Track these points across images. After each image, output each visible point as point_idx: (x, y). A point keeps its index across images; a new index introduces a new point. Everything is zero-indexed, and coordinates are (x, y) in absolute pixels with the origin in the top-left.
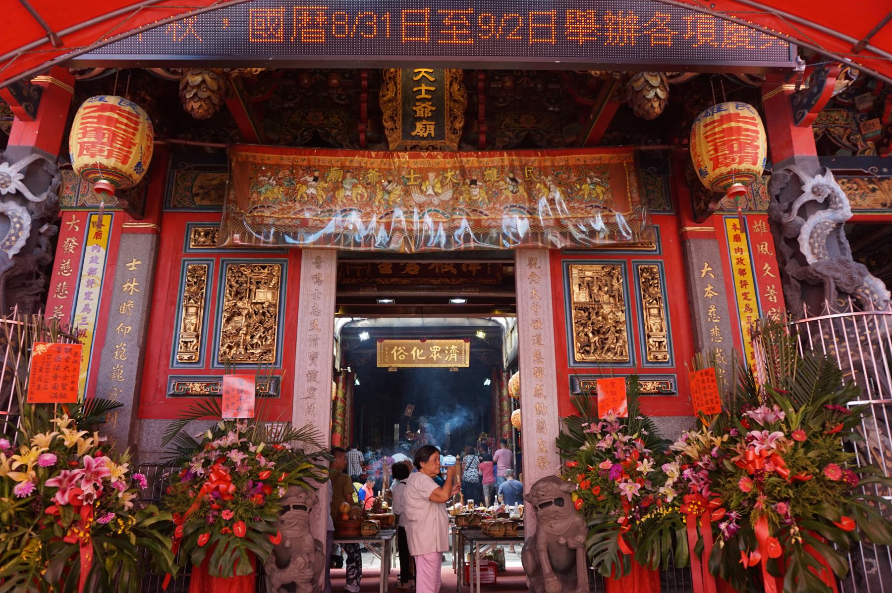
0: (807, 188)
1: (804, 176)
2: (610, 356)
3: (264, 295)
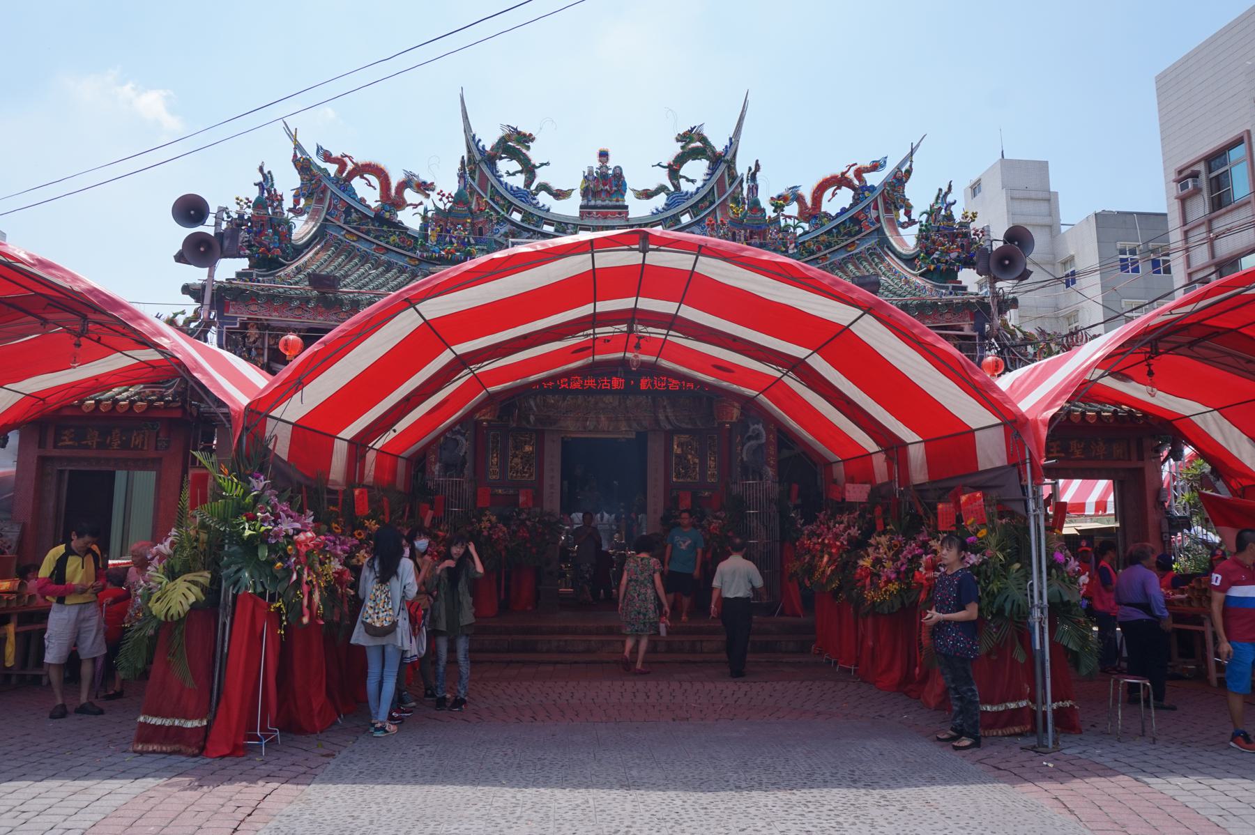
0: (751, 430)
1: (751, 425)
2: (689, 479)
3: (528, 448)
